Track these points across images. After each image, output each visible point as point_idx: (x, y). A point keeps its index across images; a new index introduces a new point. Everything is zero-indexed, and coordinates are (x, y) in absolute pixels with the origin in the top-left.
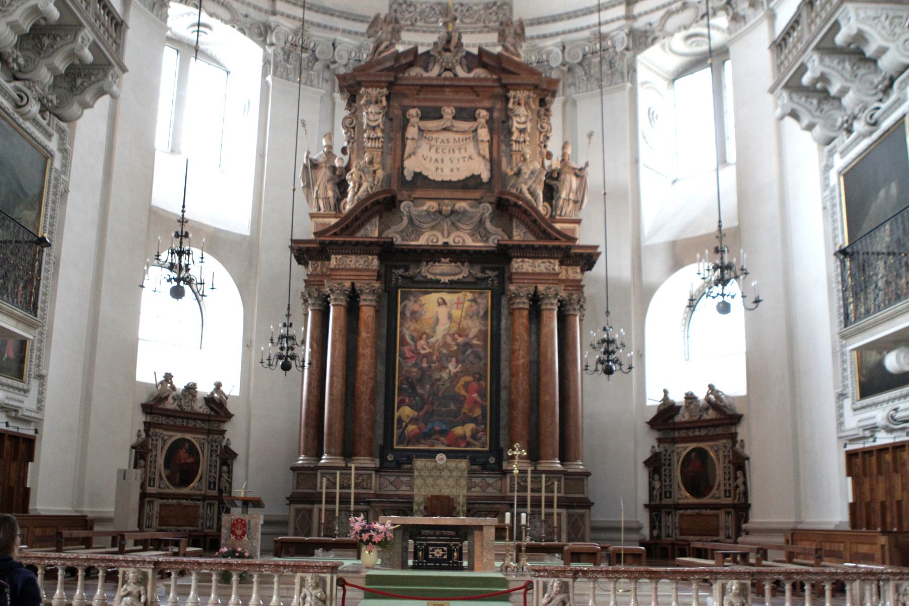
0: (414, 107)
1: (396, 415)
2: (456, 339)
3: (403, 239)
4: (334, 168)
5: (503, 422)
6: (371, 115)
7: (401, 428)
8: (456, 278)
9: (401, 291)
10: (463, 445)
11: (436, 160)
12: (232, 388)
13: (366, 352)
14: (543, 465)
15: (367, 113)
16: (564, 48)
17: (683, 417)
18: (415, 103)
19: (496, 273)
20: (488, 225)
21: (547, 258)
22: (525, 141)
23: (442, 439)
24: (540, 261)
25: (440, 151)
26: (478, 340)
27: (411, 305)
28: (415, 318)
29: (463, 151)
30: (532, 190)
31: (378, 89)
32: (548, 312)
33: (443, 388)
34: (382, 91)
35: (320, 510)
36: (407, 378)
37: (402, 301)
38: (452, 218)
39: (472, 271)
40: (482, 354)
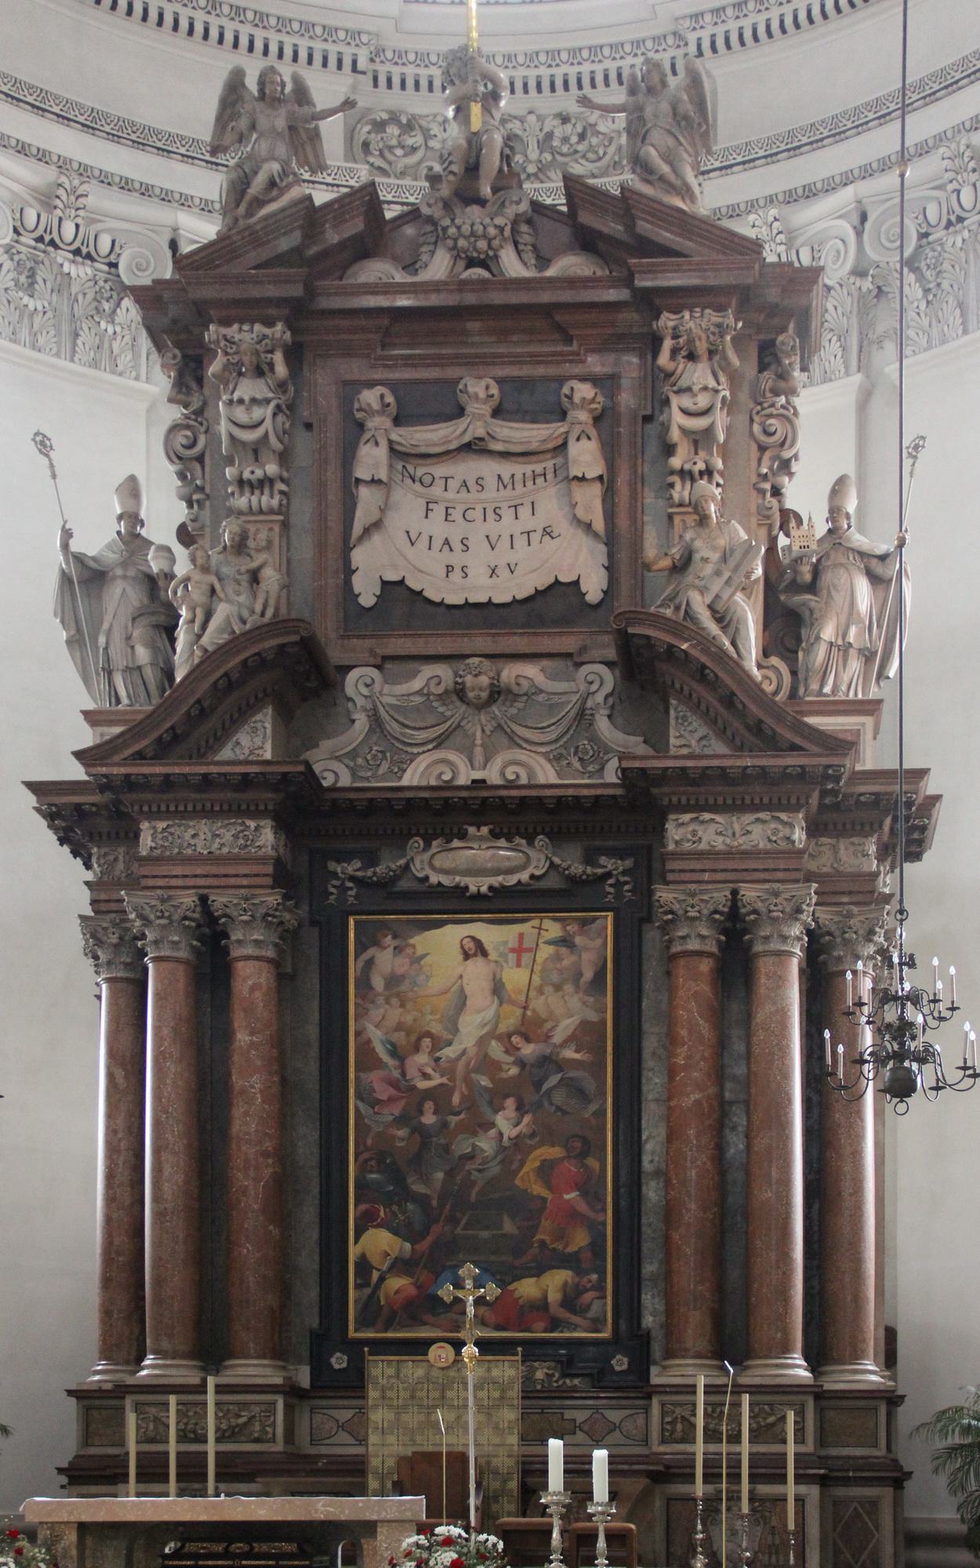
1: (353, 1252)
2: (519, 1049)
7: (368, 1285)
8: (512, 880)
9: (356, 922)
10: (541, 1325)
11: (447, 542)
14: (758, 1372)
18: (379, 375)
19: (629, 863)
20: (603, 725)
21: (769, 807)
22: (708, 473)
25: (456, 514)
26: (577, 1051)
29: (525, 512)
32: (770, 960)
33: (480, 1179)
36: (381, 1157)
37: (361, 948)
38: (495, 709)
39: (557, 860)
40: (590, 1086)
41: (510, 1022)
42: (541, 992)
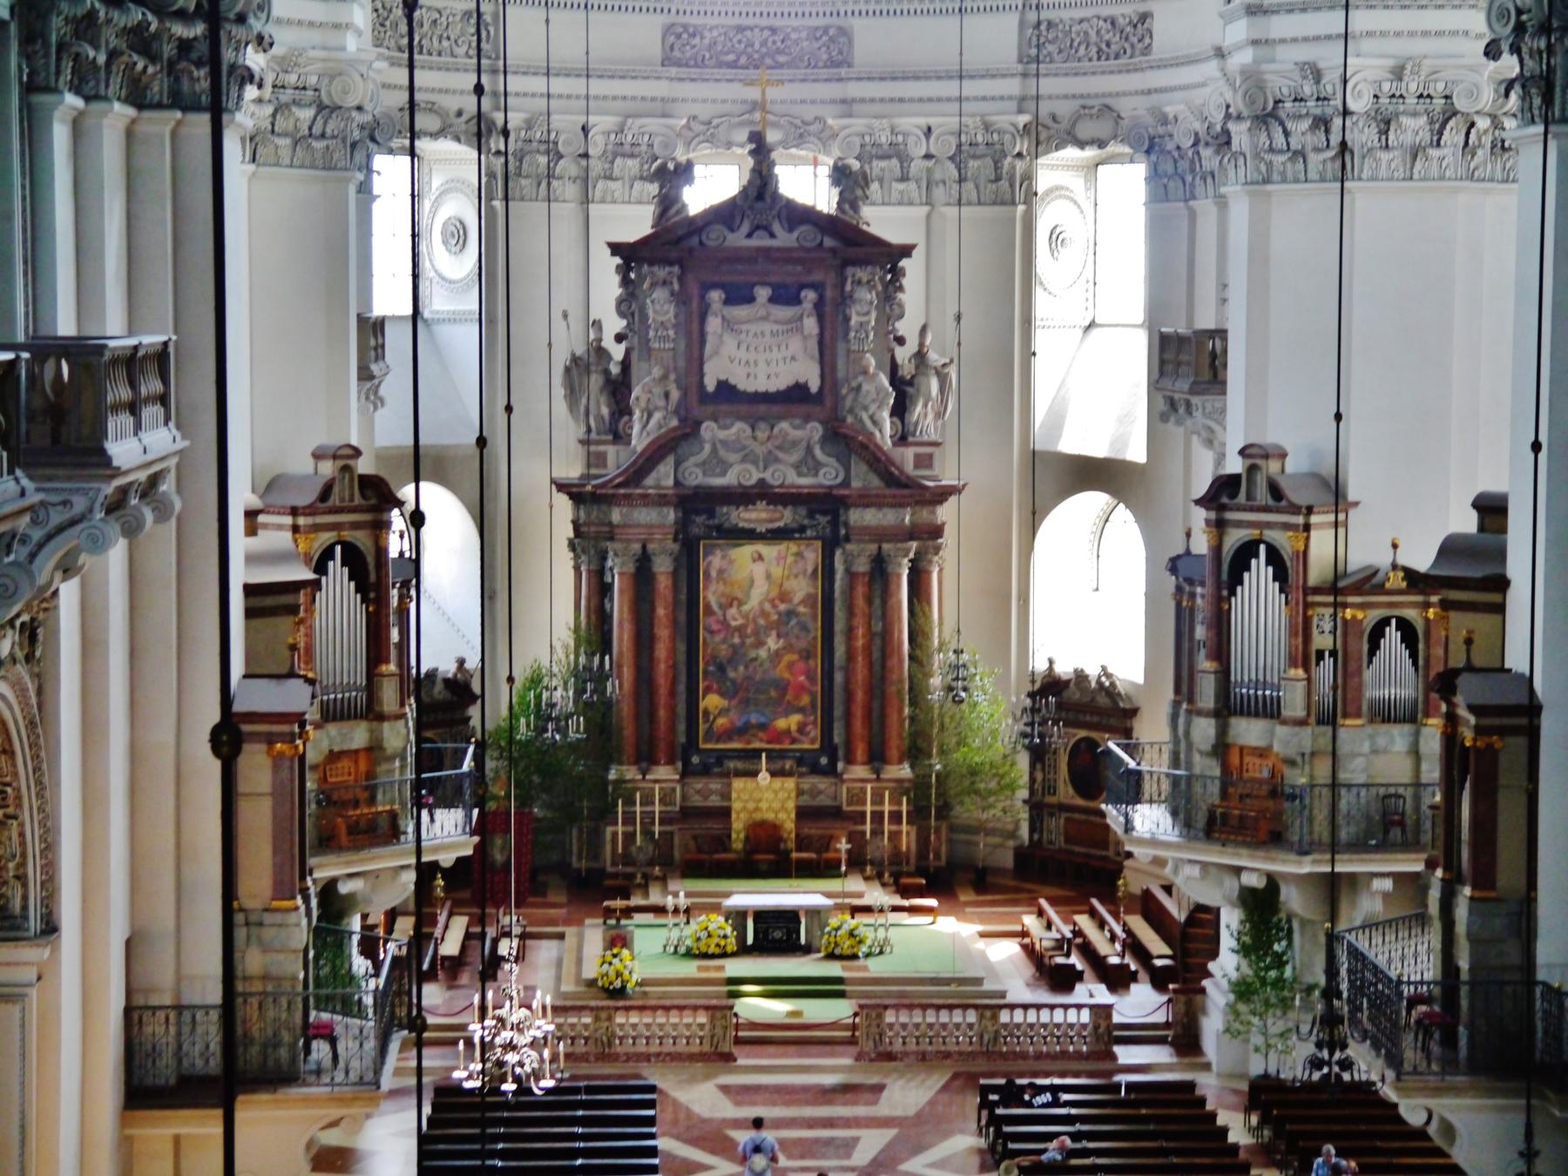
0: (715, 286)
1: (702, 705)
3: (705, 474)
4: (607, 372)
5: (838, 711)
6: (660, 306)
11: (747, 362)
13: (663, 632)
15: (653, 302)
16: (929, 129)
17: (1073, 694)
18: (716, 279)
19: (829, 518)
20: (818, 452)
23: (761, 734)
24: (886, 510)
25: (752, 348)
27: (716, 561)
28: (723, 579)
30: (876, 418)
31: (667, 269)
34: (672, 269)
35: (615, 834)
38: (770, 445)
40: (810, 625)
41: (774, 593)
42: (788, 578)
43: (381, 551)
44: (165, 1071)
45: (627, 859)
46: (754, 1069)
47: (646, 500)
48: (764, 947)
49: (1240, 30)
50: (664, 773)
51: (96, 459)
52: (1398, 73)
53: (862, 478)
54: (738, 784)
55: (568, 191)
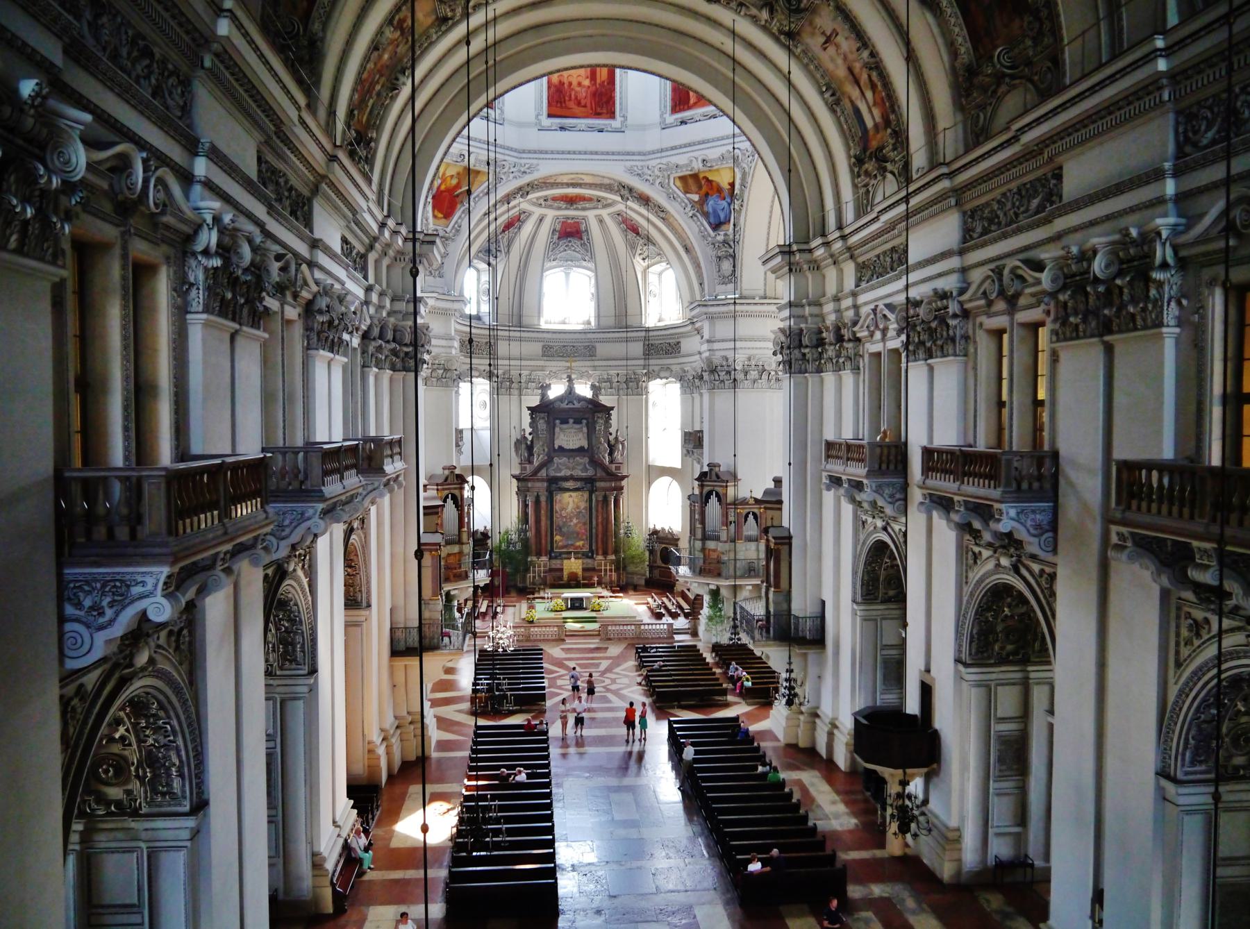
6: (542, 425)
12: (489, 527)
13: (543, 518)
17: (661, 534)
43: (462, 496)
44: (402, 647)
45: (534, 583)
46: (570, 643)
47: (538, 480)
48: (573, 608)
49: (705, 347)
50: (544, 559)
51: (380, 471)
52: (749, 359)
53: (600, 473)
54: (565, 561)
55: (516, 392)
